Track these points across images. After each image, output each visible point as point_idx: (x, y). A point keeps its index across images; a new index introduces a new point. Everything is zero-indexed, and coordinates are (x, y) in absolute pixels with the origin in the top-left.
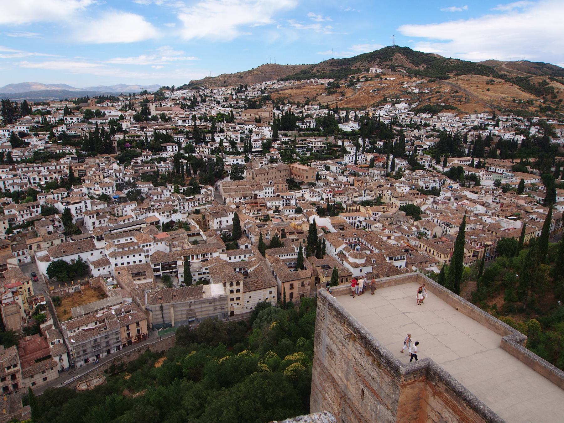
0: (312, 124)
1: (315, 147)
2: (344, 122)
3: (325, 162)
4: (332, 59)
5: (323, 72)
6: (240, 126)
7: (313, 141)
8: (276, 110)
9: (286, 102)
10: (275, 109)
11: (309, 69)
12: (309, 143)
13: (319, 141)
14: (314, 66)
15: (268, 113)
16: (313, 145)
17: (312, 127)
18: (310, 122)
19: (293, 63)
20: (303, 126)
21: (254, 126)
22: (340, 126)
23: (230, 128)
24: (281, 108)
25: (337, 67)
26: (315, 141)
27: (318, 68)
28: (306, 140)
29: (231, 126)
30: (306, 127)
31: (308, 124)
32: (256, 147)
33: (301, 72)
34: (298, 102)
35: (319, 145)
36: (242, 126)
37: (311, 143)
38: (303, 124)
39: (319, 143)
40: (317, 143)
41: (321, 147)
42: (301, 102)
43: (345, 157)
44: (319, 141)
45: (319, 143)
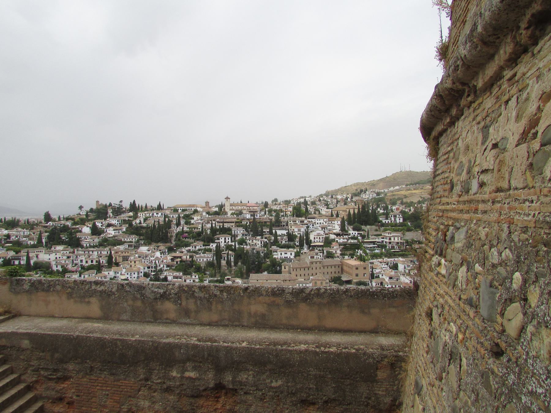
1: (390, 243)
7: (387, 235)
12: (383, 238)
13: (396, 236)
16: (388, 241)
18: (395, 216)
20: (387, 221)
21: (325, 220)
23: (297, 222)
26: (390, 235)
28: (381, 235)
30: (390, 222)
31: (393, 219)
36: (313, 220)
38: (387, 219)
39: (396, 239)
40: (392, 239)
41: (398, 243)
44: (396, 236)
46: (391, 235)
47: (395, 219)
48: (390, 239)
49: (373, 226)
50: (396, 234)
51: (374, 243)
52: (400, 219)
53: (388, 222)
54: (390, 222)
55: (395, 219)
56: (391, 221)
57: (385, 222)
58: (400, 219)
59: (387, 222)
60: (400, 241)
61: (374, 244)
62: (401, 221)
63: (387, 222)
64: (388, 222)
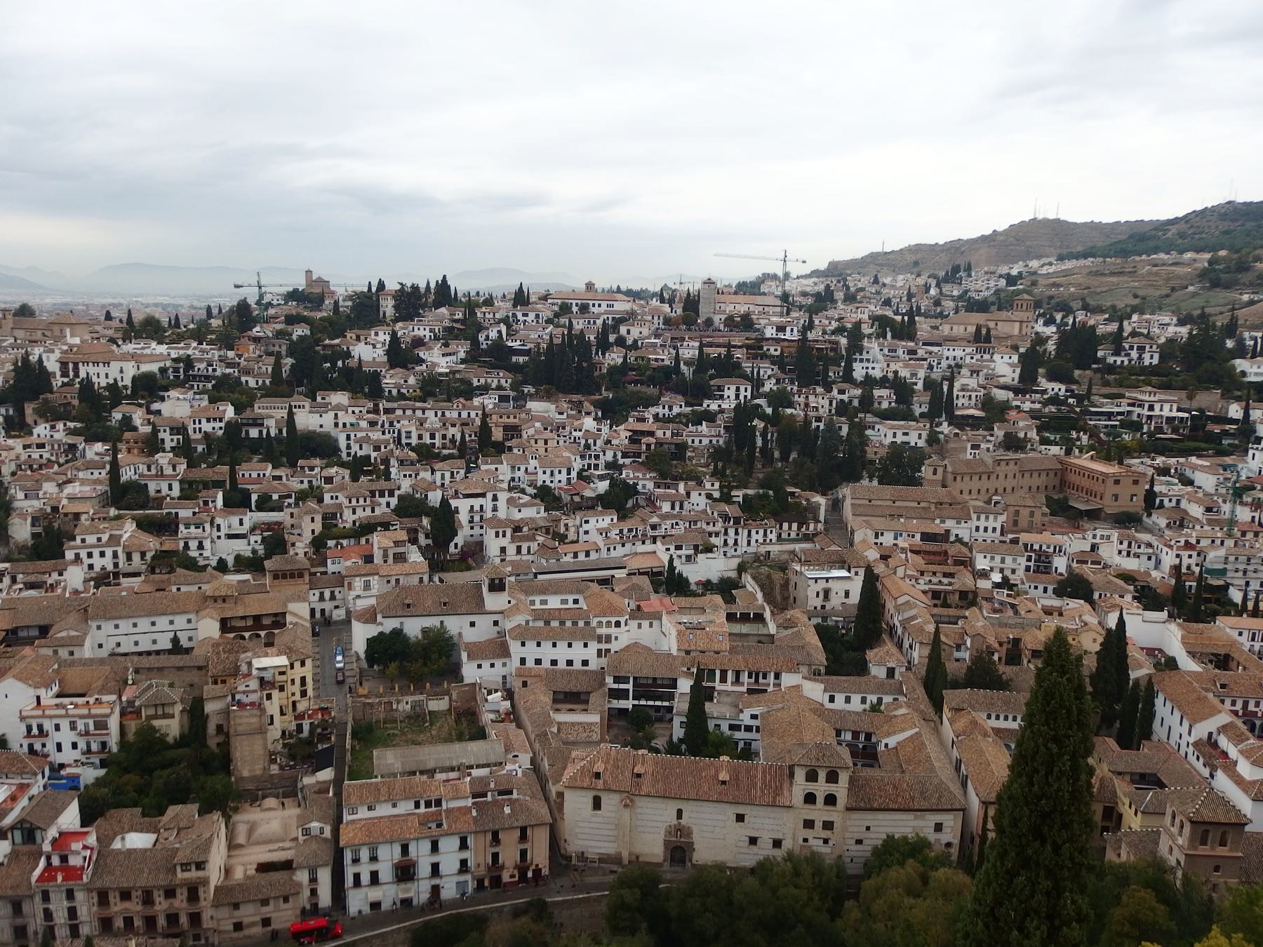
0: (1147, 356)
1: (1150, 417)
2: (1252, 357)
3: (1182, 460)
4: (1229, 203)
5: (1197, 236)
6: (930, 348)
7: (1146, 397)
8: (1046, 324)
9: (1076, 305)
10: (1041, 321)
11: (1156, 229)
12: (1133, 405)
14: (1176, 221)
15: (1017, 325)
16: (1146, 412)
17: (1147, 363)
18: (1141, 349)
19: (1107, 218)
20: (1119, 360)
21: (969, 350)
22: (1241, 364)
23: (900, 352)
24: (1058, 321)
25: (1243, 225)
26: (1152, 398)
27: (1182, 226)
28: (1123, 396)
30: (1126, 363)
31: (1134, 354)
32: (966, 404)
33: (1131, 237)
34: (1114, 307)
35: (1166, 412)
36: (935, 349)
37: (1140, 406)
38: (1117, 353)
39: (1167, 407)
40: (1157, 407)
41: (1170, 420)
42: (1120, 305)
43: (1251, 452)
45: (1167, 407)
46: (1156, 399)
47: (1140, 356)
48: (1151, 408)
49: (1088, 372)
50: (1163, 397)
51: (1109, 415)
52: (1152, 357)
53: (1122, 362)
54: (1126, 363)
55: (1140, 356)
56: (1130, 361)
57: (1115, 361)
58: (1152, 357)
59: (1119, 363)
60: (1175, 414)
61: (1110, 420)
62: (1155, 361)
63: (1119, 363)
64: (1122, 362)
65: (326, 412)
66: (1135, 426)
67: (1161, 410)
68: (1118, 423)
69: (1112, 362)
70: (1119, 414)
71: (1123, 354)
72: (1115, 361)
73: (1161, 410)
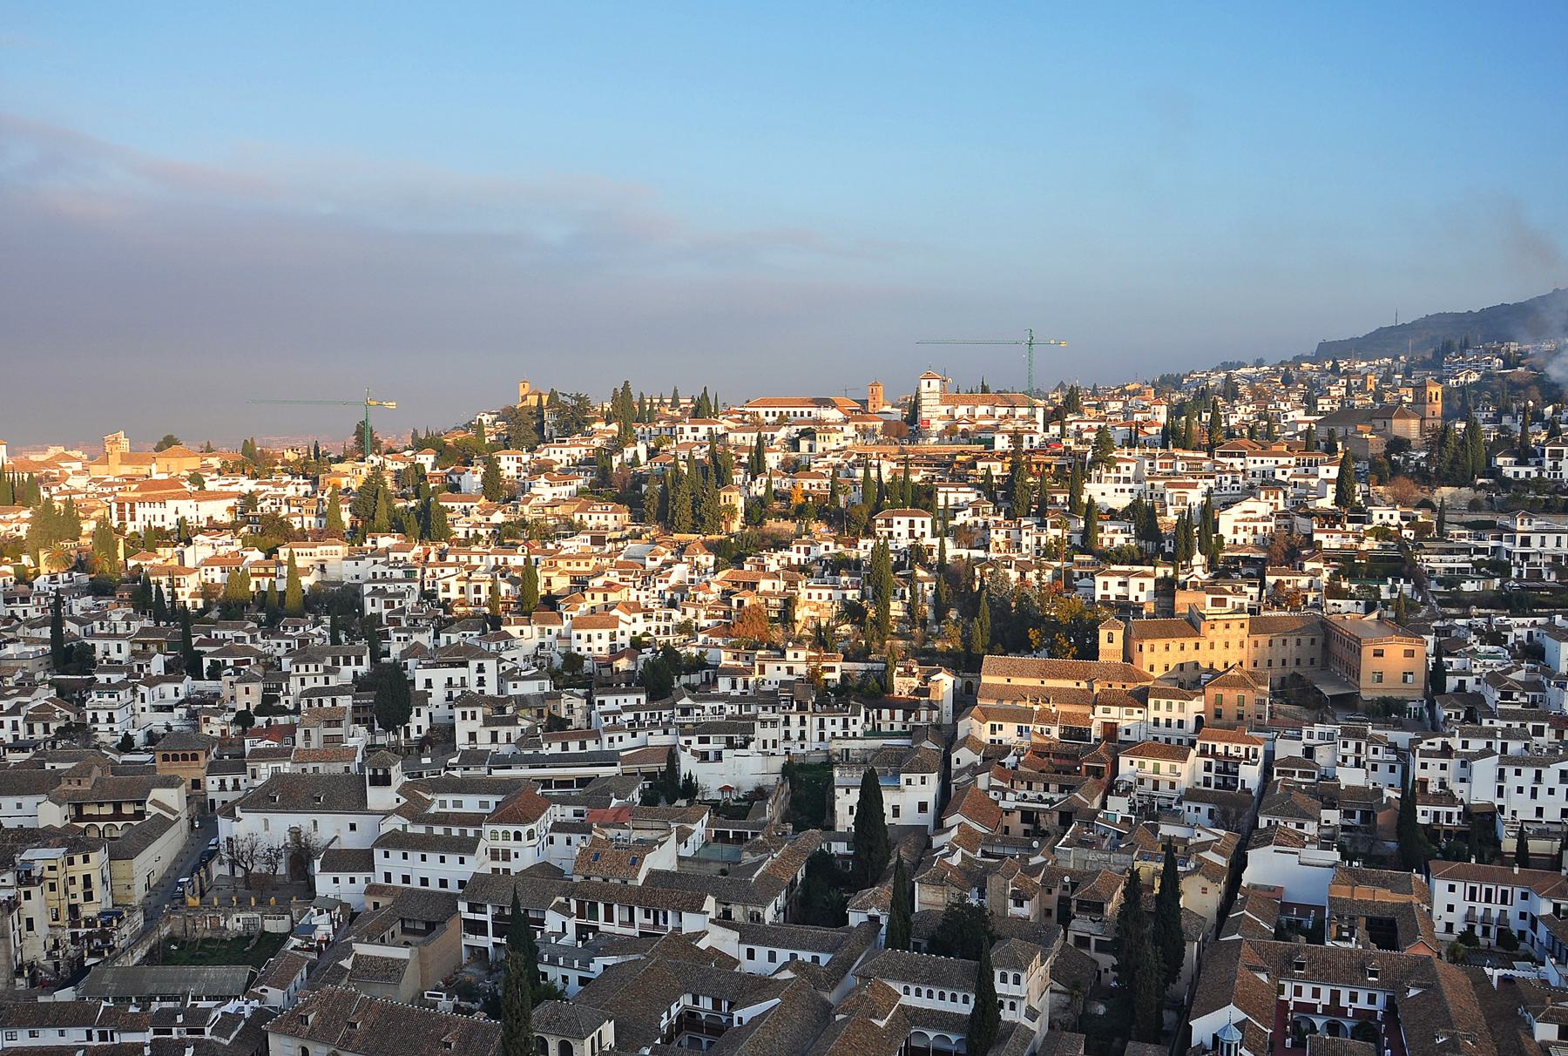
1: (1525, 556)
16: (1518, 549)
20: (1522, 471)
29: (1182, 458)
30: (1534, 474)
36: (1237, 462)
38: (1521, 462)
40: (1535, 540)
48: (1526, 542)
53: (1528, 474)
57: (1516, 474)
63: (1522, 475)
64: (1528, 474)
65: (363, 559)
66: (1501, 568)
67: (1543, 545)
68: (1470, 565)
69: (1511, 475)
70: (1478, 551)
71: (1532, 461)
72: (1516, 474)
73: (1543, 545)
